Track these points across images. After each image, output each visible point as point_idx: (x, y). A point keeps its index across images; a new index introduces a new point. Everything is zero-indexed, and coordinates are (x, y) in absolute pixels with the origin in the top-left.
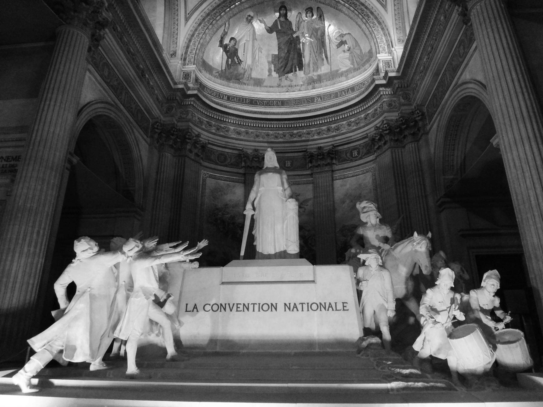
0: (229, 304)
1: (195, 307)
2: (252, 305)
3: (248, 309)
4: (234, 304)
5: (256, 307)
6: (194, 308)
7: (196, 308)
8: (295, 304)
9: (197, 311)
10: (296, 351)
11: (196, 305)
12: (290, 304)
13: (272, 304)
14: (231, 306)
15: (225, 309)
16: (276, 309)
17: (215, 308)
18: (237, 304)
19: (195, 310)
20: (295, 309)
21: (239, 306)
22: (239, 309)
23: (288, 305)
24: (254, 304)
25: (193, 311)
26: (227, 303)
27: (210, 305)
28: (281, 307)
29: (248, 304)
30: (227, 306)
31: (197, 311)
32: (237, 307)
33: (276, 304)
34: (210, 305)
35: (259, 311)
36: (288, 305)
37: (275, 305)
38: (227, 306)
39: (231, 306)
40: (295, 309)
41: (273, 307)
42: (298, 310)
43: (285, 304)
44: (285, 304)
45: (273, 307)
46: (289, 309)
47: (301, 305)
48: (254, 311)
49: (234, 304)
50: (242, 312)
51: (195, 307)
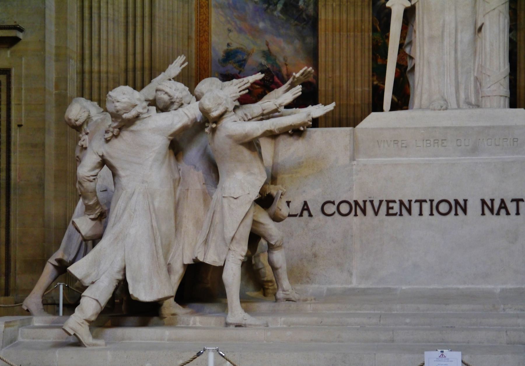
0: (372, 202)
1: (305, 207)
2: (418, 204)
3: (409, 211)
4: (381, 202)
5: (426, 207)
6: (303, 209)
7: (308, 209)
8: (502, 201)
9: (310, 215)
10: (504, 286)
11: (305, 203)
12: (492, 201)
13: (457, 202)
14: (376, 204)
15: (364, 212)
16: (465, 211)
17: (345, 209)
18: (388, 202)
19: (306, 213)
20: (503, 211)
21: (391, 205)
22: (391, 211)
23: (489, 203)
24: (421, 202)
25: (301, 215)
26: (368, 199)
27: (333, 203)
28: (474, 207)
29: (410, 201)
30: (368, 204)
31: (310, 215)
32: (389, 208)
33: (465, 201)
34: (333, 203)
35: (432, 214)
36: (489, 203)
37: (462, 203)
38: (368, 204)
39: (376, 204)
40: (503, 211)
41: (460, 207)
42: (508, 213)
43: (483, 202)
44: (483, 202)
45: (460, 207)
46: (492, 210)
47: (515, 203)
48: (421, 214)
49: (381, 202)
50: (397, 217)
51: (305, 207)
